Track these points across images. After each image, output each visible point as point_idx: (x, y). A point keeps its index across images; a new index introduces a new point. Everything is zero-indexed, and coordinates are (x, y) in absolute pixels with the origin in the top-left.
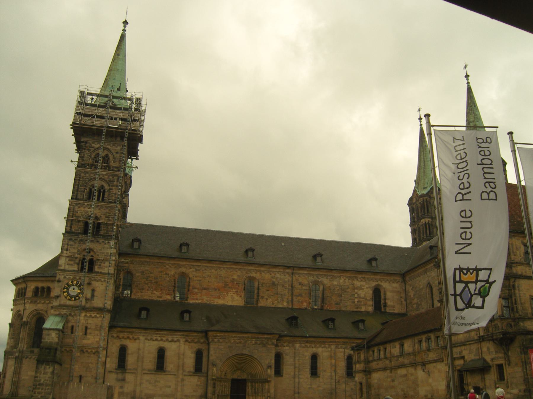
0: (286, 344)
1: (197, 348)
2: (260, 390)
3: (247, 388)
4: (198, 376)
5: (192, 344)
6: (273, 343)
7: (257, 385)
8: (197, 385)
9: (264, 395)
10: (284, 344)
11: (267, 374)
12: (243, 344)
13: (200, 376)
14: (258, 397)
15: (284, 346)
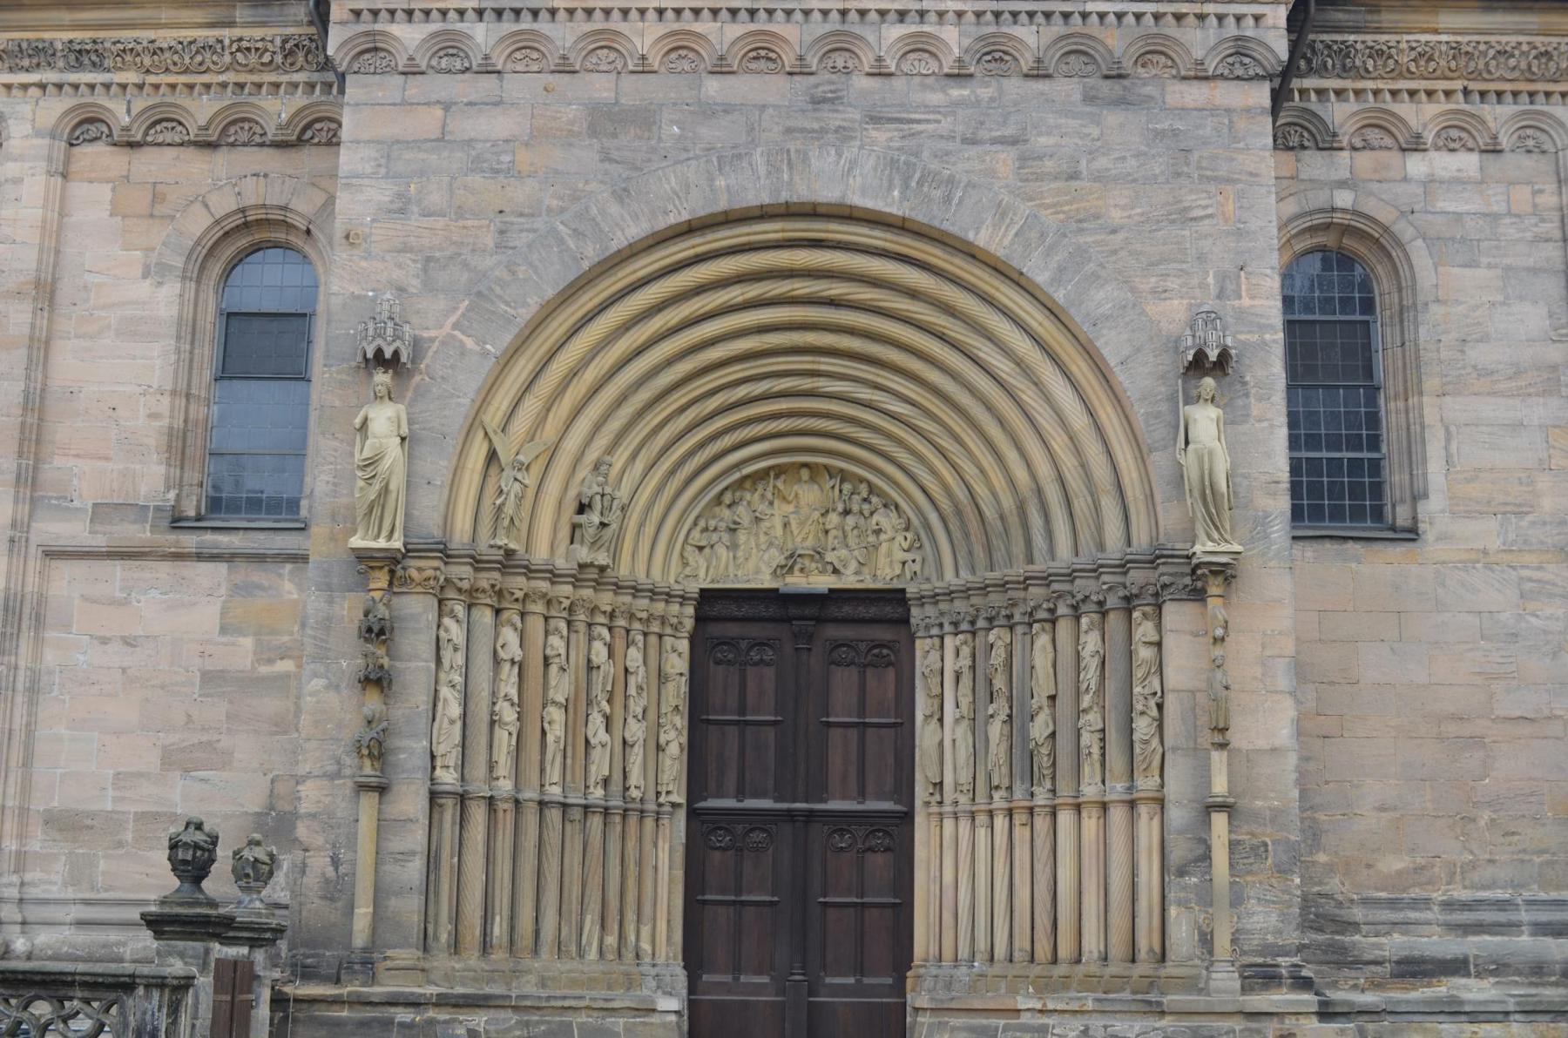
0: (1431, 109)
1: (225, 204)
2: (1093, 719)
3: (922, 706)
4: (230, 557)
5: (153, 164)
6: (1241, 49)
7: (1042, 660)
8: (212, 679)
9: (1146, 783)
10: (1404, 109)
11: (1178, 478)
12: (800, 70)
13: (259, 558)
14: (1065, 818)
15: (1415, 145)
